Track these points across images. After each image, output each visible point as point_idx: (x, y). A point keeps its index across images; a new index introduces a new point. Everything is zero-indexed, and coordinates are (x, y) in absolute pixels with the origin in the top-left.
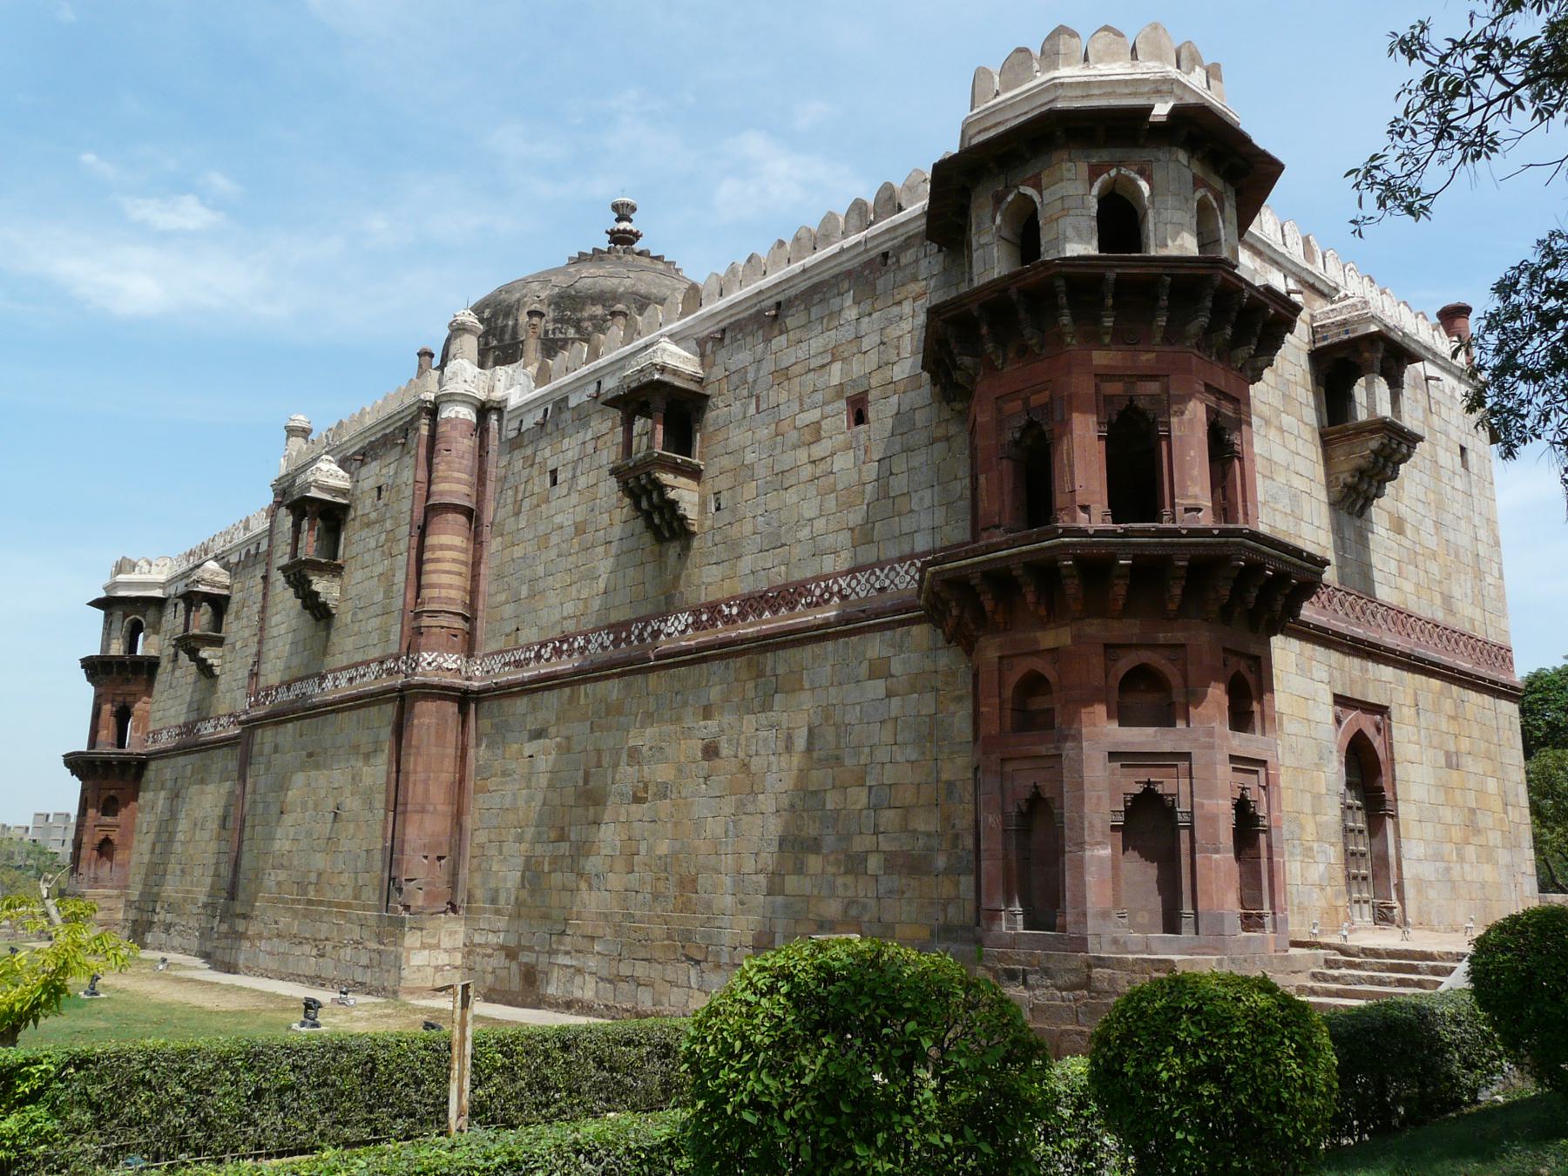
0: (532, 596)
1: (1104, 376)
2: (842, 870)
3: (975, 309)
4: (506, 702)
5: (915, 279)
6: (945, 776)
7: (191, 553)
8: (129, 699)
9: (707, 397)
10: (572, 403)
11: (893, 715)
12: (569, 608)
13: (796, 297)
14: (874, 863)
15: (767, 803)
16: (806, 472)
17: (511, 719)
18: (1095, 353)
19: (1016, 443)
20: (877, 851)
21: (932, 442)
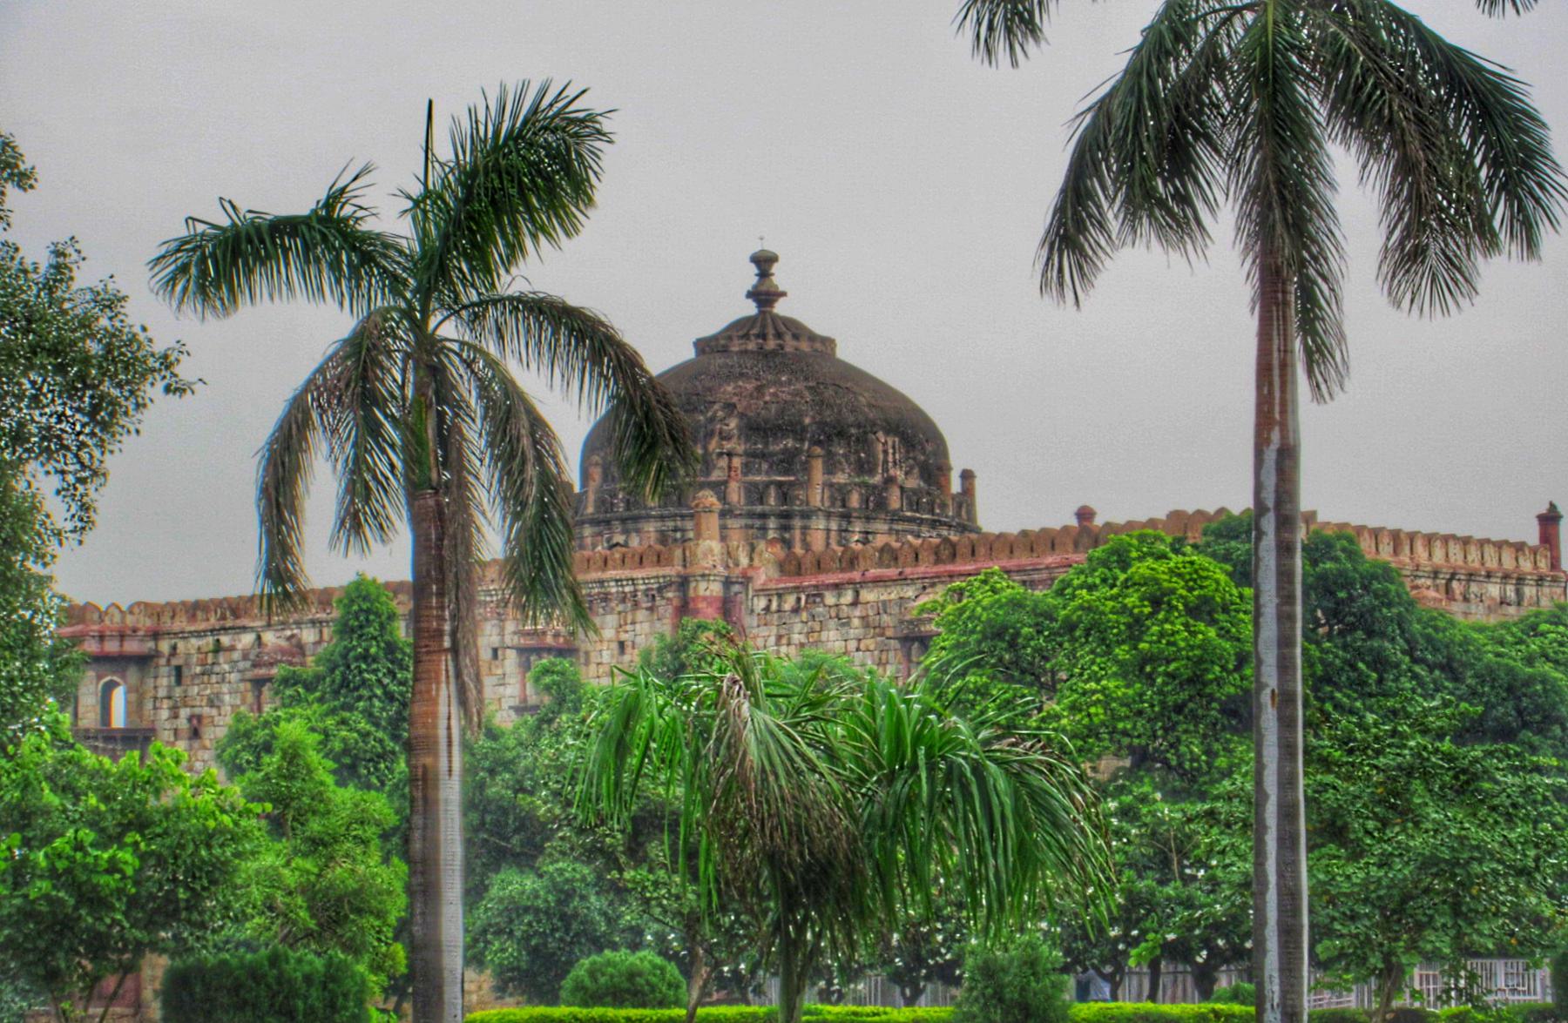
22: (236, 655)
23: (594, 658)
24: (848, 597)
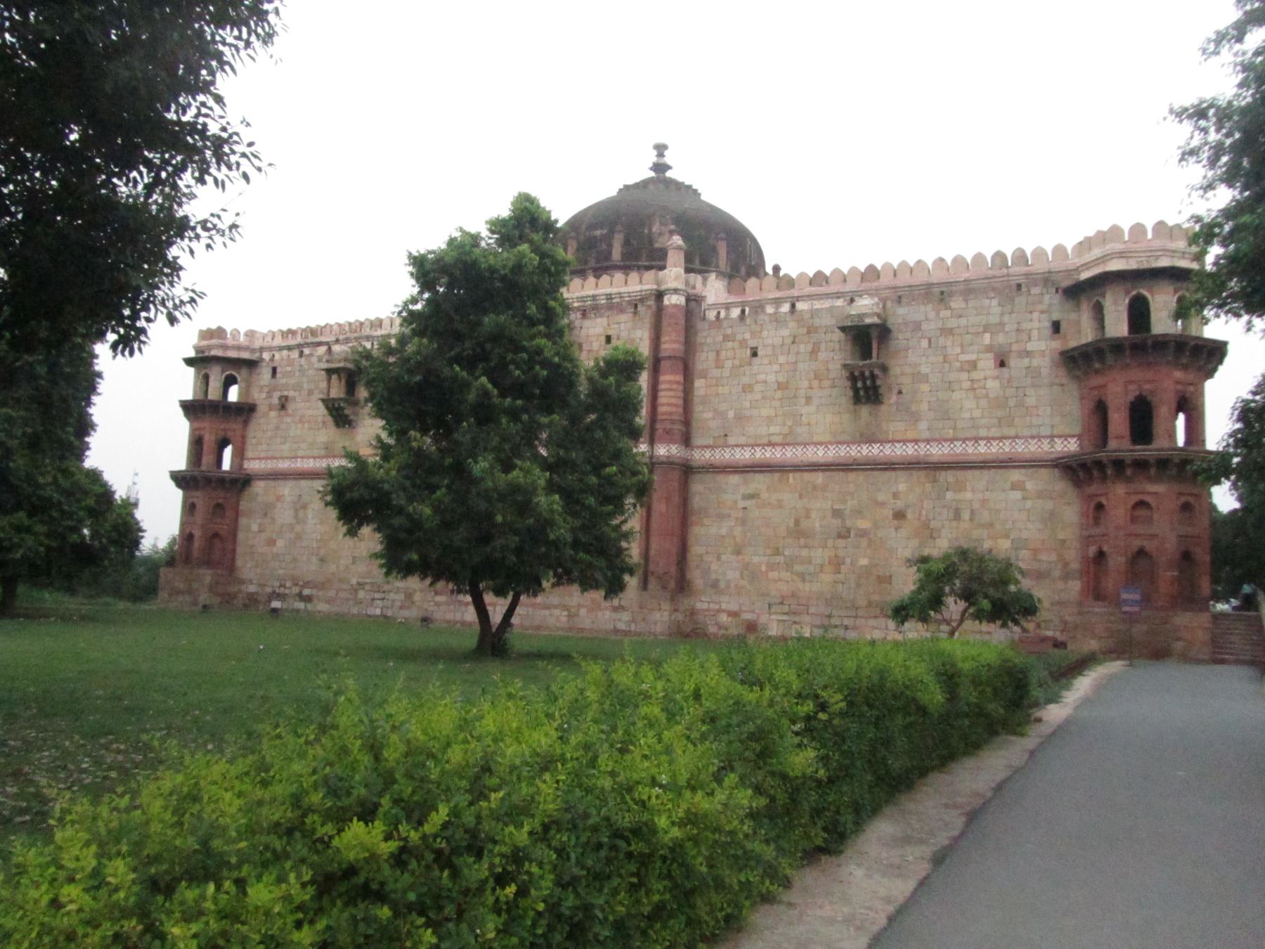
0: (739, 418)
1: (1178, 383)
3: (1127, 343)
4: (721, 478)
5: (1041, 302)
6: (1061, 536)
7: (292, 332)
8: (230, 434)
12: (773, 429)
19: (1132, 403)
21: (1052, 385)
22: (314, 359)
23: (585, 347)
24: (786, 308)
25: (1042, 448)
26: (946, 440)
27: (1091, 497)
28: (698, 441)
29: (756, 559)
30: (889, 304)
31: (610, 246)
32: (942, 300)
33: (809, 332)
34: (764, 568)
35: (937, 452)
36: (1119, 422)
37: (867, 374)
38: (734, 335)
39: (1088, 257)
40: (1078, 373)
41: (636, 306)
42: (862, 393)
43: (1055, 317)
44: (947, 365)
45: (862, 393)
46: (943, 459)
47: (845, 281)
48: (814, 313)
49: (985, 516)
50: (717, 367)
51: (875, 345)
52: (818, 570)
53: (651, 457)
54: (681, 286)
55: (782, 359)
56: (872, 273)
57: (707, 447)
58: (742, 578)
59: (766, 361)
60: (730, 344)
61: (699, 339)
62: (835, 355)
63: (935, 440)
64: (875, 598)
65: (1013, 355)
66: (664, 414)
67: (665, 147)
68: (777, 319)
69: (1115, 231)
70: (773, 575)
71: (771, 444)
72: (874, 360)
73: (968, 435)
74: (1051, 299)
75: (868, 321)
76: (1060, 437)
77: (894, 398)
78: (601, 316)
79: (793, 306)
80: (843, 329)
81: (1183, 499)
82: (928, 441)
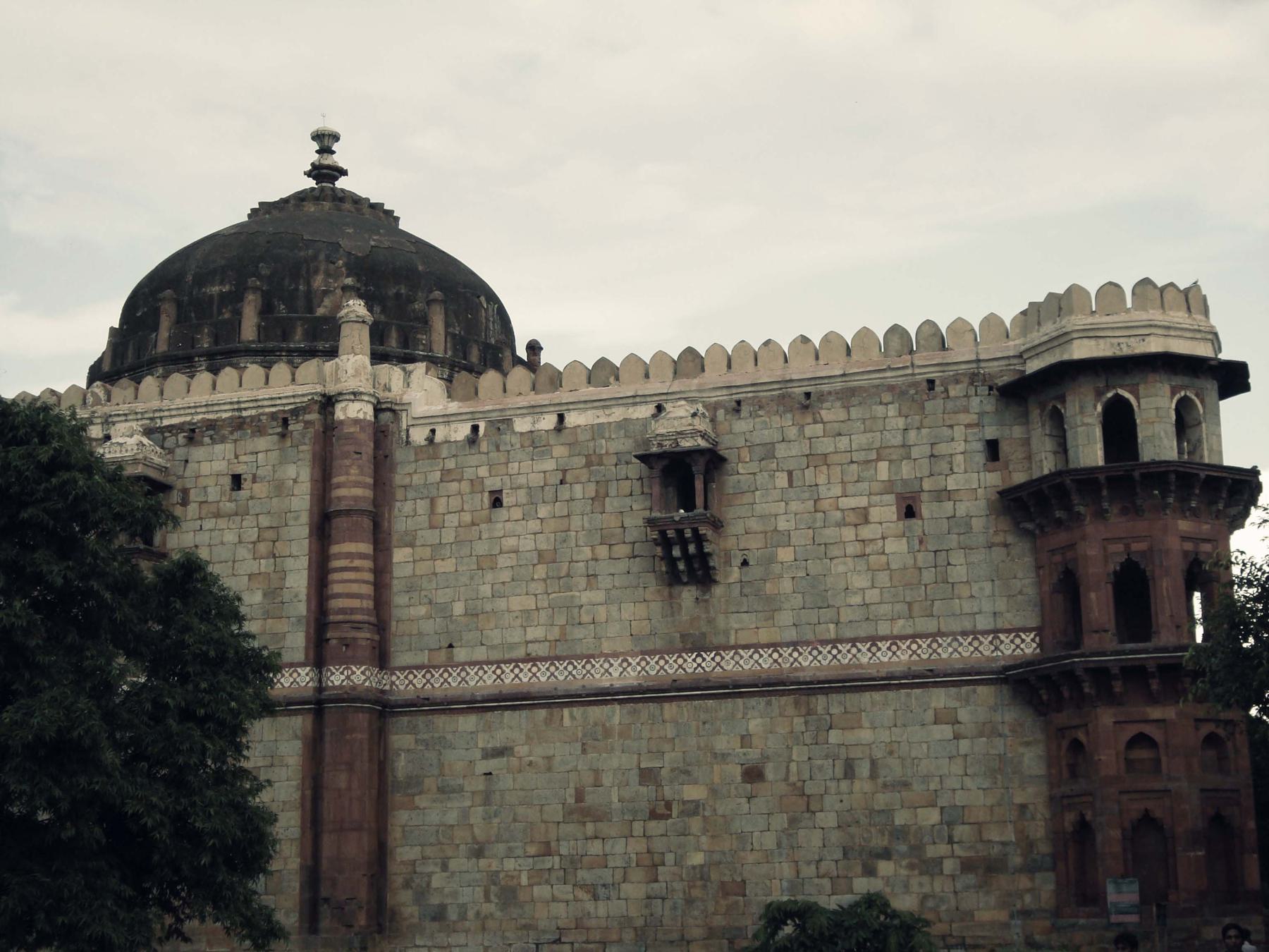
0: (471, 614)
1: (1184, 538)
2: (916, 872)
4: (441, 721)
5: (966, 410)
6: (1018, 800)
9: (723, 460)
10: (522, 425)
11: (962, 752)
12: (534, 633)
13: (830, 393)
14: (949, 866)
15: (828, 819)
16: (850, 550)
17: (449, 737)
18: (1180, 522)
19: (1115, 572)
20: (953, 856)
21: (990, 546)
24: (549, 422)
25: (985, 651)
26: (824, 642)
27: (1062, 731)
28: (401, 657)
29: (510, 864)
30: (721, 413)
31: (238, 314)
32: (806, 407)
33: (588, 464)
34: (524, 880)
35: (809, 662)
36: (1099, 605)
37: (688, 534)
38: (461, 468)
39: (1036, 337)
40: (1030, 526)
41: (285, 422)
42: (681, 566)
43: (991, 433)
44: (820, 515)
45: (681, 566)
46: (822, 675)
47: (647, 376)
48: (597, 431)
49: (893, 769)
50: (432, 527)
51: (699, 485)
52: (619, 876)
53: (320, 689)
54: (364, 385)
55: (543, 511)
56: (690, 362)
57: (419, 668)
58: (488, 900)
59: (517, 513)
60: (455, 485)
61: (399, 478)
62: (632, 508)
63: (807, 643)
64: (719, 921)
65: (925, 497)
66: (343, 611)
67: (336, 138)
68: (533, 441)
69: (1075, 291)
70: (542, 891)
71: (529, 659)
72: (700, 510)
73: (863, 634)
74: (982, 403)
75: (686, 444)
76: (1008, 631)
77: (735, 574)
78: (223, 440)
79: (561, 418)
80: (643, 458)
81: (1206, 729)
82: (795, 645)
